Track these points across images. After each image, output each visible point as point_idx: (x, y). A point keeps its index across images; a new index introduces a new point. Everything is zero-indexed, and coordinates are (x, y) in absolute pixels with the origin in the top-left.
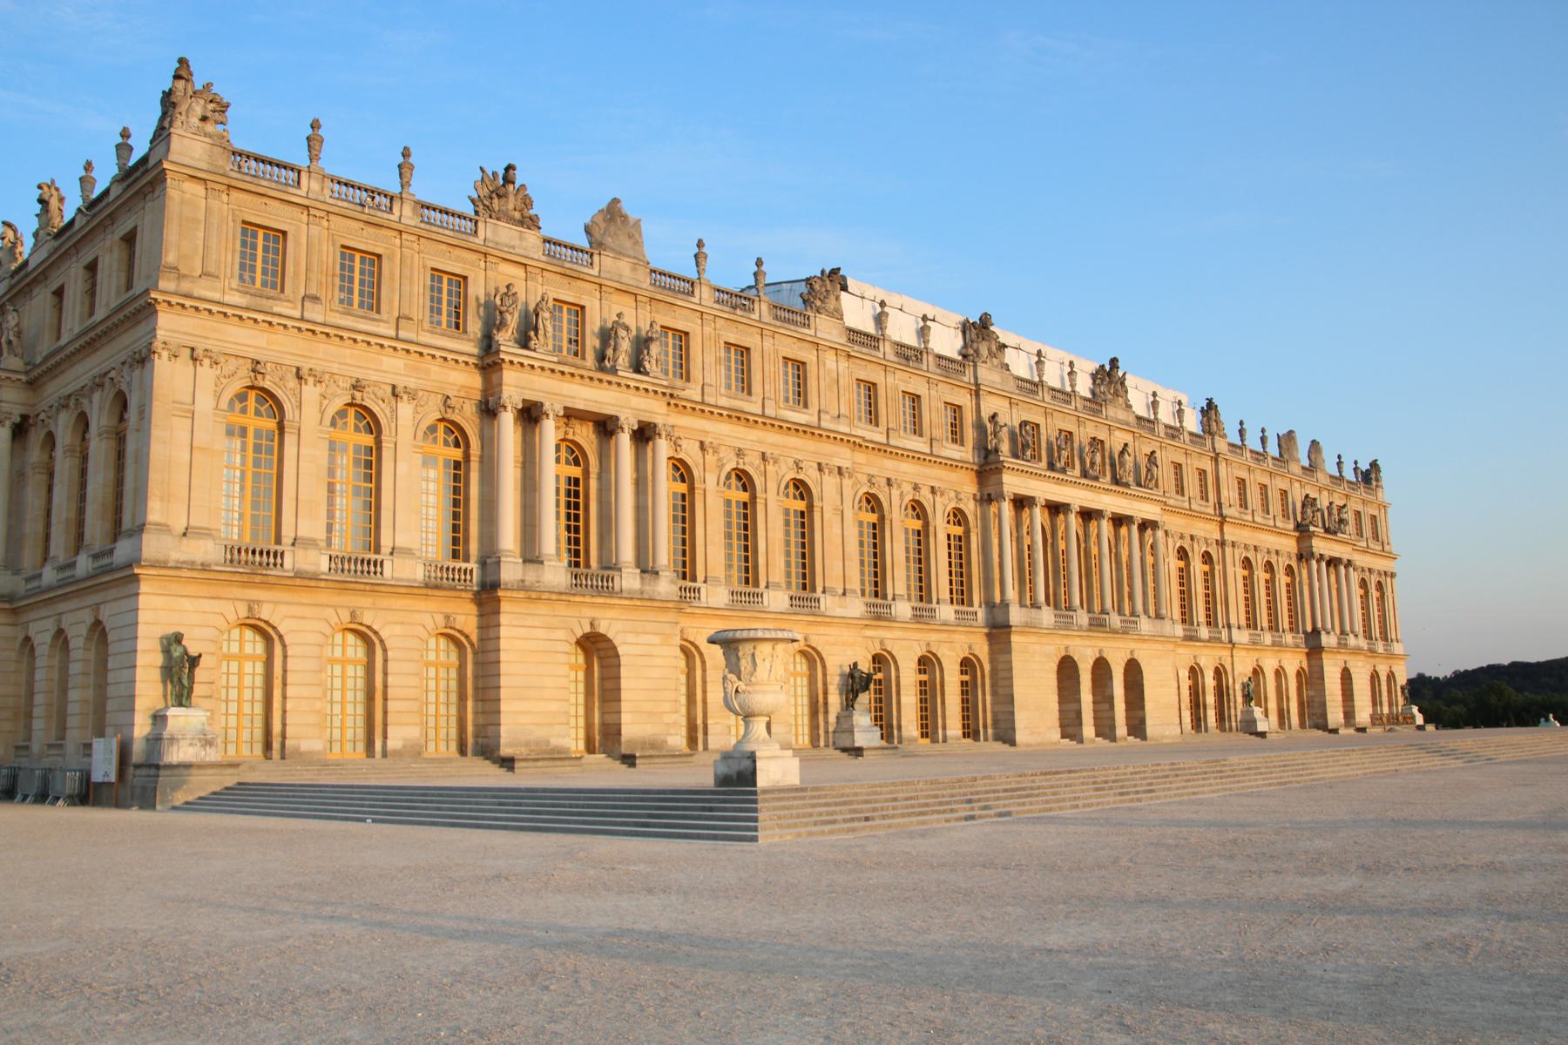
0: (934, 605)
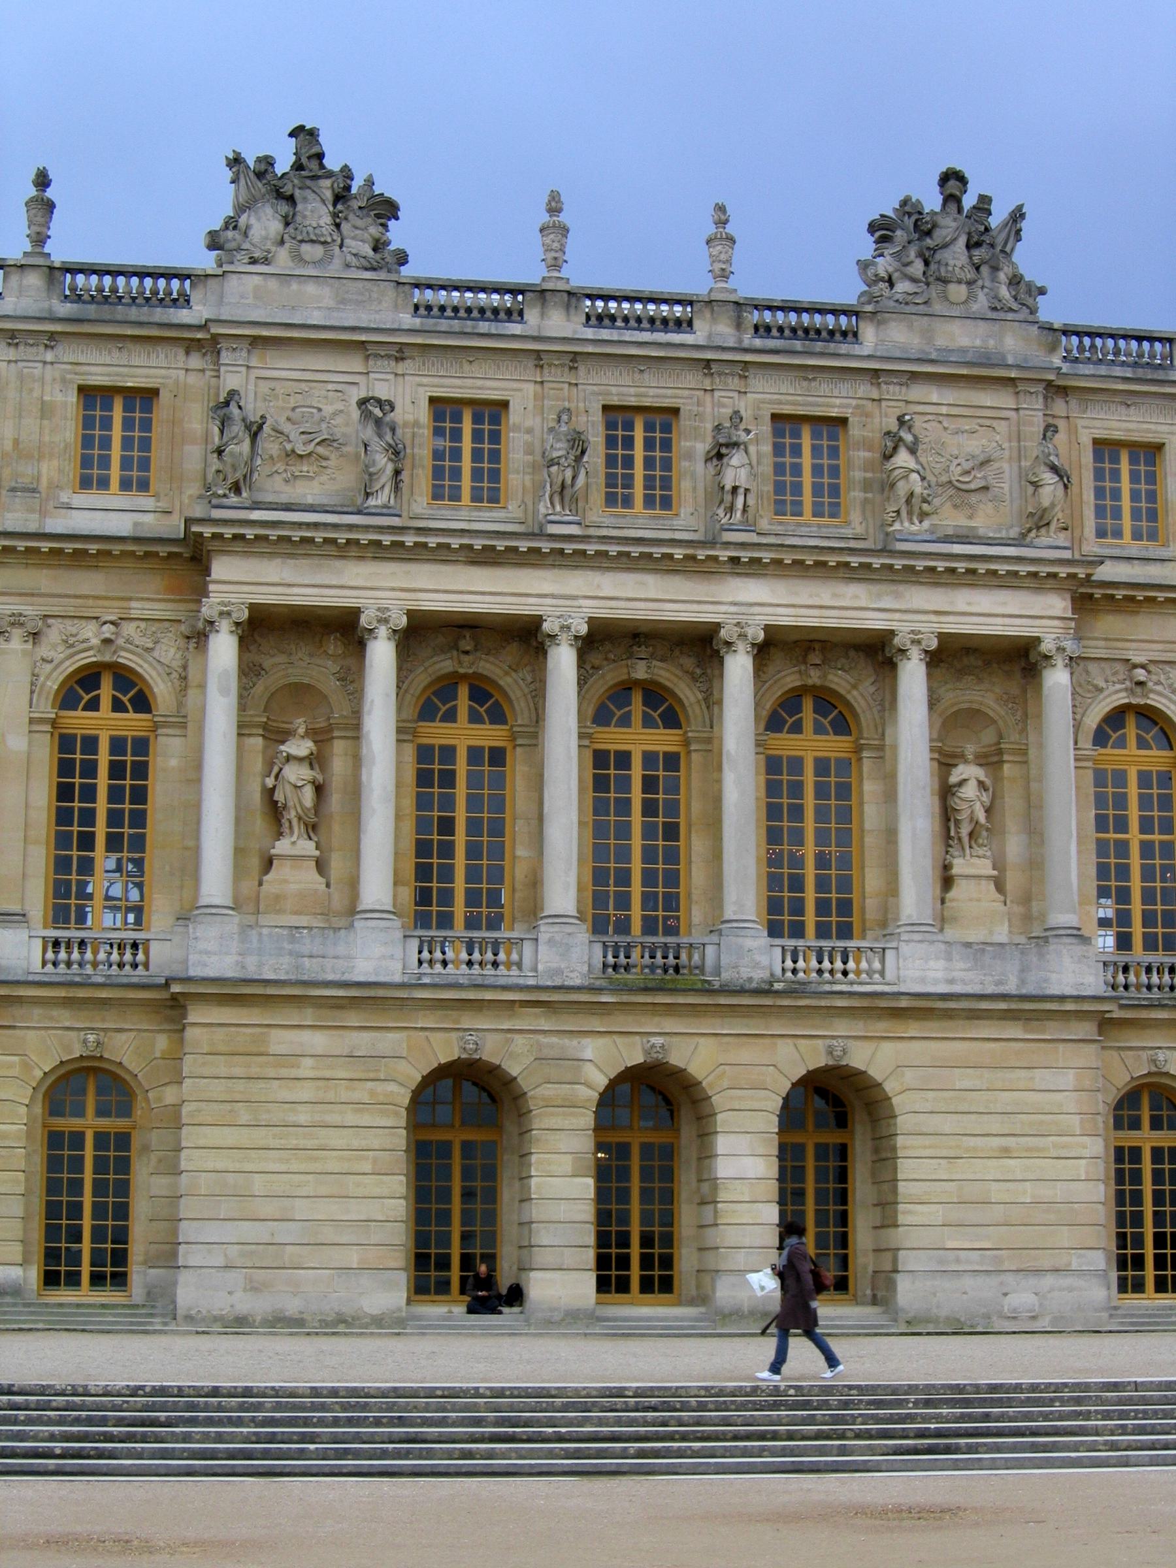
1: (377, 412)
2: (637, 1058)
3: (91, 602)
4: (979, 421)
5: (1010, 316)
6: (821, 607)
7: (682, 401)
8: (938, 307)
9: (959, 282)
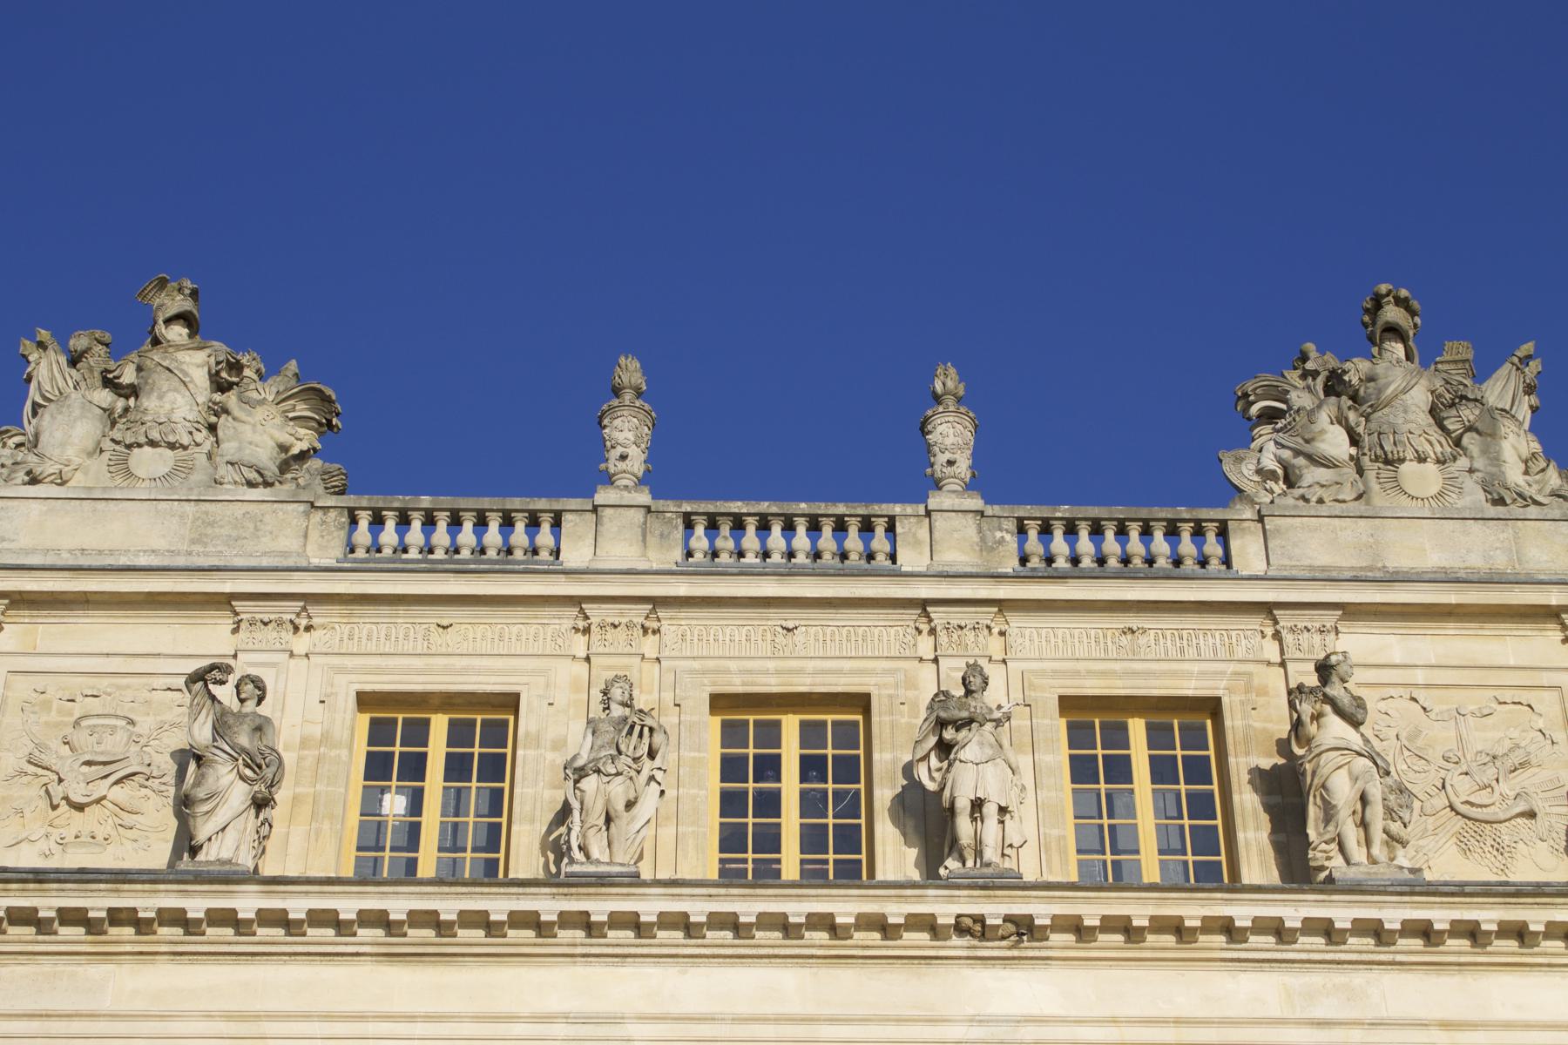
1: (225, 693)
4: (1498, 693)
5: (1533, 511)
6: (1178, 1022)
7: (873, 680)
8: (1379, 499)
9: (1422, 459)
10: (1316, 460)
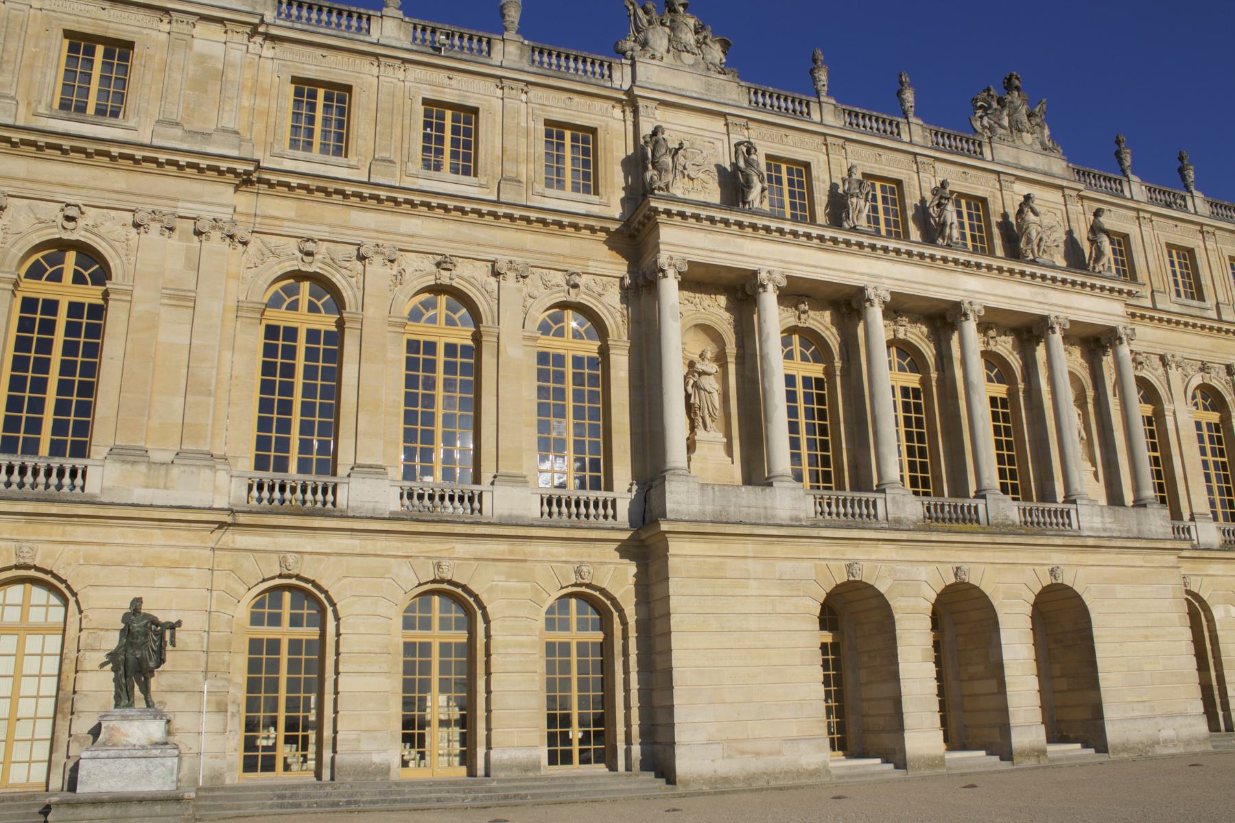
0: (485, 485)
2: (951, 580)
3: (562, 259)
8: (1018, 143)
10: (1001, 126)
